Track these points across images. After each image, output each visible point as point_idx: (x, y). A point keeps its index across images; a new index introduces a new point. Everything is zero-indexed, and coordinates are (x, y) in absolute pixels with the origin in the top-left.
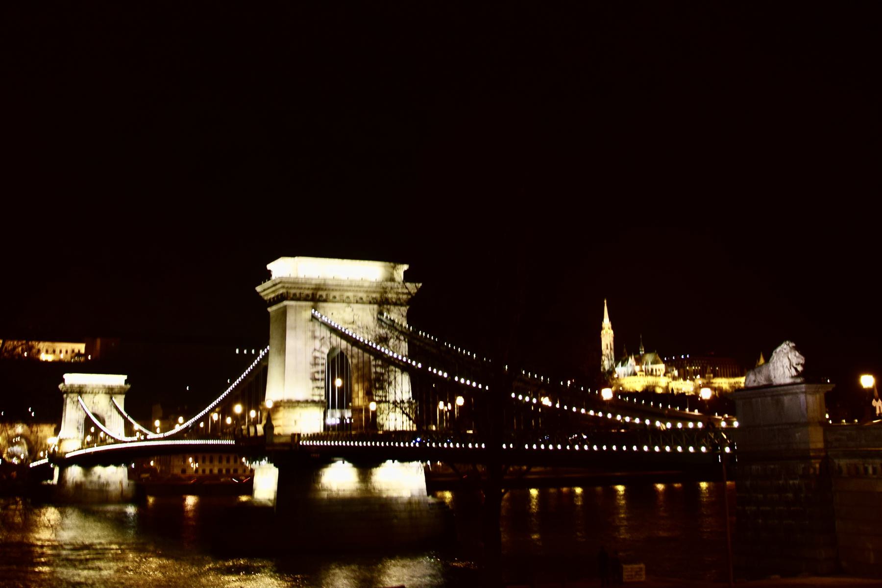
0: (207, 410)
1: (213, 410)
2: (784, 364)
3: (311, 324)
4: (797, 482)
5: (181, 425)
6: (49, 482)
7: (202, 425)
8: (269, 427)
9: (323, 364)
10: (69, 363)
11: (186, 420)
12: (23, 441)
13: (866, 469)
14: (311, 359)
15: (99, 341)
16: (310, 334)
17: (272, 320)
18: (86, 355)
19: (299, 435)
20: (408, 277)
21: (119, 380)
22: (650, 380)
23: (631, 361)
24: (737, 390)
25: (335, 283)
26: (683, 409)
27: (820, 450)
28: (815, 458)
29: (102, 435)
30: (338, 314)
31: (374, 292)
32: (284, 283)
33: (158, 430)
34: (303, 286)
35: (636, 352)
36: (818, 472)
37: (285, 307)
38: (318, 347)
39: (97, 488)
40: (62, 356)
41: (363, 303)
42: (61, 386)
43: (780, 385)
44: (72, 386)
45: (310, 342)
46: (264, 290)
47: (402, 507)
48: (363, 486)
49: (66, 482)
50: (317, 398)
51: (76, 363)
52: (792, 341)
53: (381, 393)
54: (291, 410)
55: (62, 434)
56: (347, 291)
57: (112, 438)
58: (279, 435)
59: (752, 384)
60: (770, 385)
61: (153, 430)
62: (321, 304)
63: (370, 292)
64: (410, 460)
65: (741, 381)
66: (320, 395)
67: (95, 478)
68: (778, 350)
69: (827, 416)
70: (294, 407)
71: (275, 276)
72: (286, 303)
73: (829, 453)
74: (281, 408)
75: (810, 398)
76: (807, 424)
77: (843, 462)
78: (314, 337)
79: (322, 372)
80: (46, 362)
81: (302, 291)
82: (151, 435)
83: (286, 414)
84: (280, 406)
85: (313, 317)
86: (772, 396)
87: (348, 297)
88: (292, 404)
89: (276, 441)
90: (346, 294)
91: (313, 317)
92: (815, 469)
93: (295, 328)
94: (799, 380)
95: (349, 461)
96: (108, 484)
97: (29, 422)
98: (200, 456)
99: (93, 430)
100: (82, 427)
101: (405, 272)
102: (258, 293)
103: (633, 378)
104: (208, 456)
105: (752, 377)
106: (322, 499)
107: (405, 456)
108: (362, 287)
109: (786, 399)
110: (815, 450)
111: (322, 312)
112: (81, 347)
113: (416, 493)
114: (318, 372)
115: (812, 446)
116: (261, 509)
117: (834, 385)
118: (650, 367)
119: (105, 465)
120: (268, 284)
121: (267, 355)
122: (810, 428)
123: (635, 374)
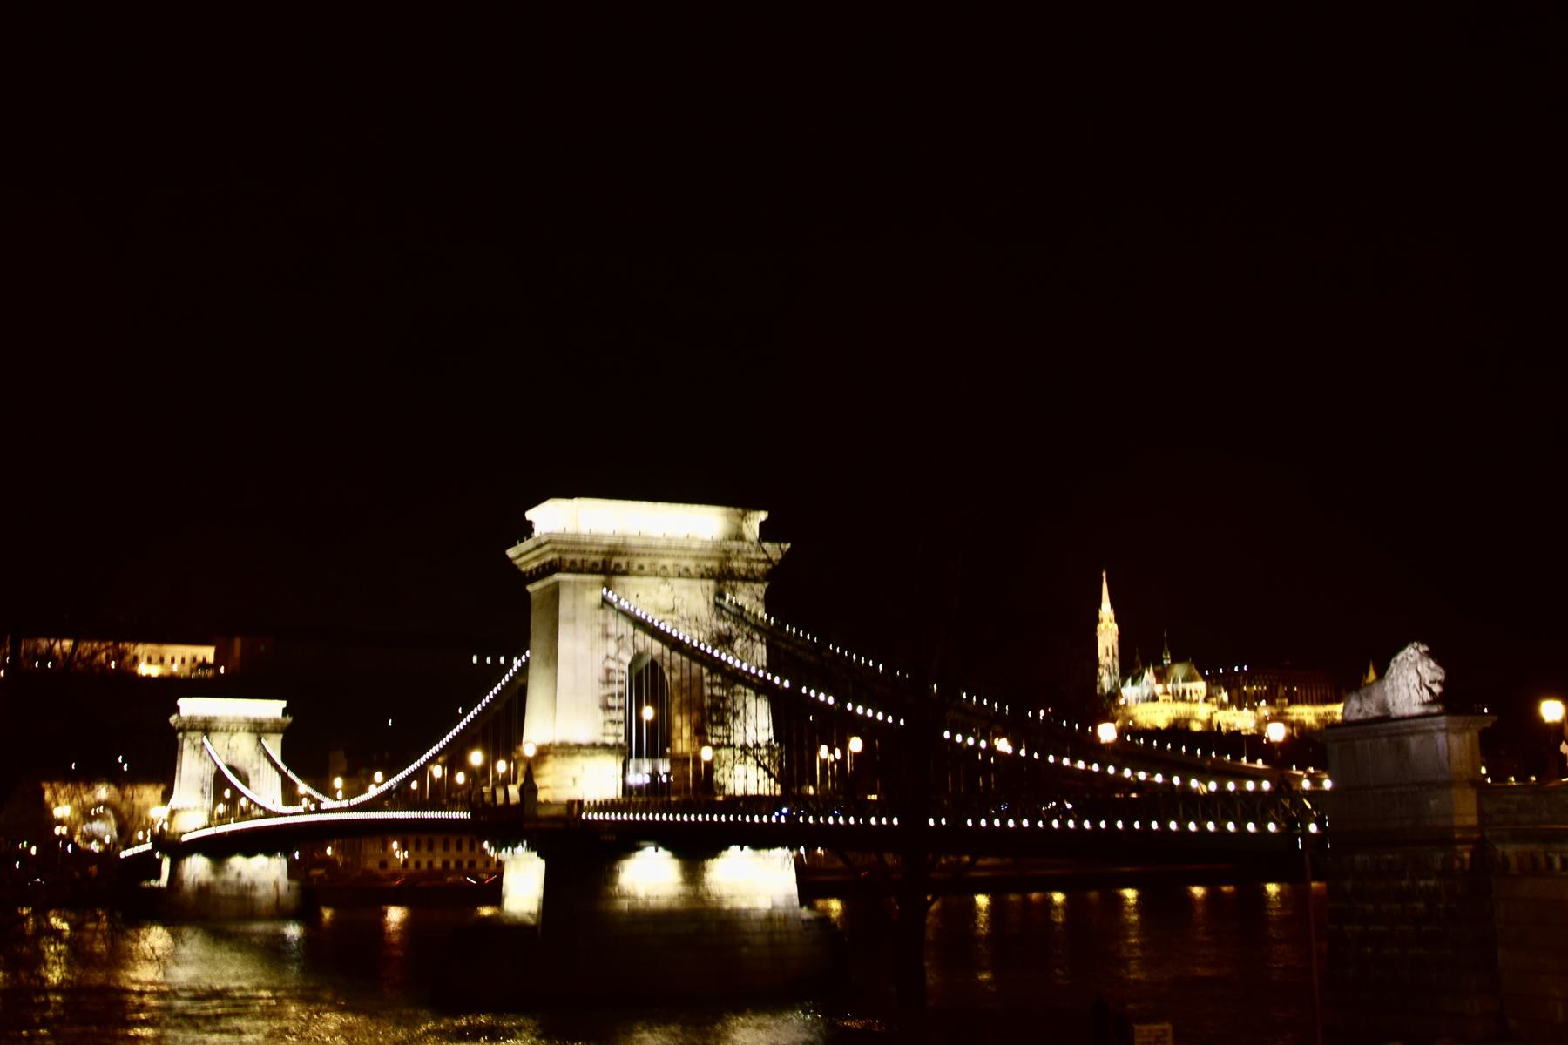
0: (423, 759)
1: (433, 760)
2: (1411, 681)
3: (601, 613)
4: (1431, 883)
5: (378, 785)
6: (153, 882)
7: (414, 785)
8: (529, 789)
9: (621, 682)
10: (187, 679)
11: (387, 778)
12: (109, 812)
13: (1550, 862)
14: (600, 673)
15: (238, 643)
16: (599, 630)
17: (535, 606)
18: (215, 666)
19: (580, 803)
20: (766, 532)
21: (272, 709)
22: (1181, 709)
23: (1149, 676)
24: (1329, 726)
25: (641, 542)
26: (1236, 758)
27: (1471, 828)
28: (1463, 841)
29: (243, 802)
30: (645, 596)
31: (709, 558)
32: (555, 542)
33: (340, 795)
34: (588, 548)
35: (1157, 662)
36: (1467, 866)
37: (557, 583)
38: (612, 652)
39: (235, 893)
40: (175, 668)
41: (690, 577)
42: (173, 719)
43: (1404, 718)
44: (192, 719)
45: (600, 644)
46: (521, 555)
47: (757, 927)
48: (689, 890)
49: (182, 883)
50: (611, 740)
51: (198, 679)
52: (1423, 642)
53: (720, 731)
54: (567, 760)
55: (175, 801)
56: (662, 556)
57: (261, 808)
58: (547, 803)
59: (1355, 716)
60: (1385, 718)
61: (331, 793)
62: (618, 580)
63: (703, 558)
64: (770, 845)
65: (1337, 710)
66: (617, 735)
67: (231, 876)
68: (1399, 657)
69: (1484, 771)
70: (571, 755)
71: (539, 530)
72: (558, 577)
73: (1487, 834)
74: (550, 757)
75: (1455, 741)
76: (1448, 784)
77: (1511, 849)
78: (607, 636)
79: (620, 695)
80: (148, 677)
81: (585, 557)
82: (327, 803)
83: (558, 768)
84: (548, 753)
85: (605, 602)
86: (1390, 736)
87: (664, 567)
88: (568, 750)
89: (542, 812)
90: (662, 562)
91: (605, 602)
92: (1462, 860)
93: (574, 619)
94: (1435, 709)
95: (667, 848)
96: (253, 887)
97: (119, 780)
98: (411, 839)
99: (227, 793)
100: (209, 790)
101: (762, 525)
102: (510, 561)
103: (1151, 705)
104: (424, 839)
105: (1355, 704)
106: (621, 913)
107: (761, 839)
108: (688, 549)
109: (1413, 741)
110: (1462, 829)
111: (620, 593)
112: (208, 653)
113: (780, 901)
114: (613, 695)
115: (1458, 822)
116: (515, 929)
117: (1495, 718)
118: (1180, 686)
119: (249, 854)
120: (528, 544)
121: (525, 666)
122: (1454, 791)
123: (1155, 699)
